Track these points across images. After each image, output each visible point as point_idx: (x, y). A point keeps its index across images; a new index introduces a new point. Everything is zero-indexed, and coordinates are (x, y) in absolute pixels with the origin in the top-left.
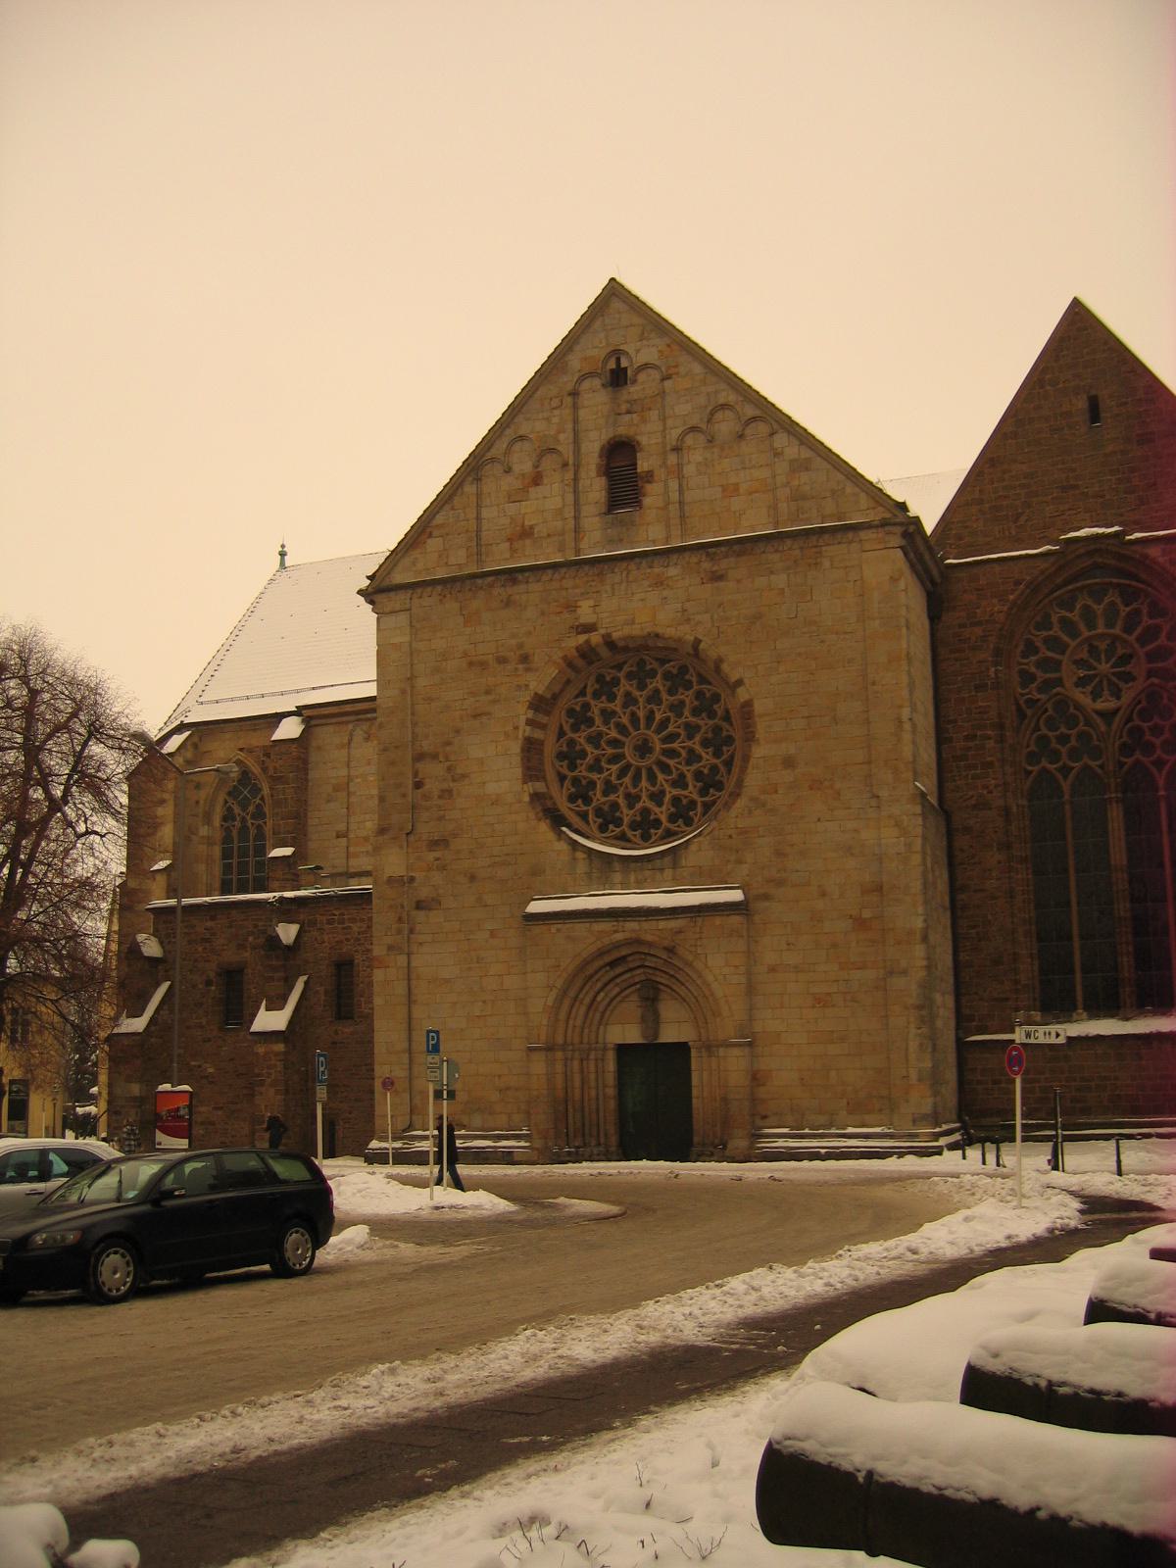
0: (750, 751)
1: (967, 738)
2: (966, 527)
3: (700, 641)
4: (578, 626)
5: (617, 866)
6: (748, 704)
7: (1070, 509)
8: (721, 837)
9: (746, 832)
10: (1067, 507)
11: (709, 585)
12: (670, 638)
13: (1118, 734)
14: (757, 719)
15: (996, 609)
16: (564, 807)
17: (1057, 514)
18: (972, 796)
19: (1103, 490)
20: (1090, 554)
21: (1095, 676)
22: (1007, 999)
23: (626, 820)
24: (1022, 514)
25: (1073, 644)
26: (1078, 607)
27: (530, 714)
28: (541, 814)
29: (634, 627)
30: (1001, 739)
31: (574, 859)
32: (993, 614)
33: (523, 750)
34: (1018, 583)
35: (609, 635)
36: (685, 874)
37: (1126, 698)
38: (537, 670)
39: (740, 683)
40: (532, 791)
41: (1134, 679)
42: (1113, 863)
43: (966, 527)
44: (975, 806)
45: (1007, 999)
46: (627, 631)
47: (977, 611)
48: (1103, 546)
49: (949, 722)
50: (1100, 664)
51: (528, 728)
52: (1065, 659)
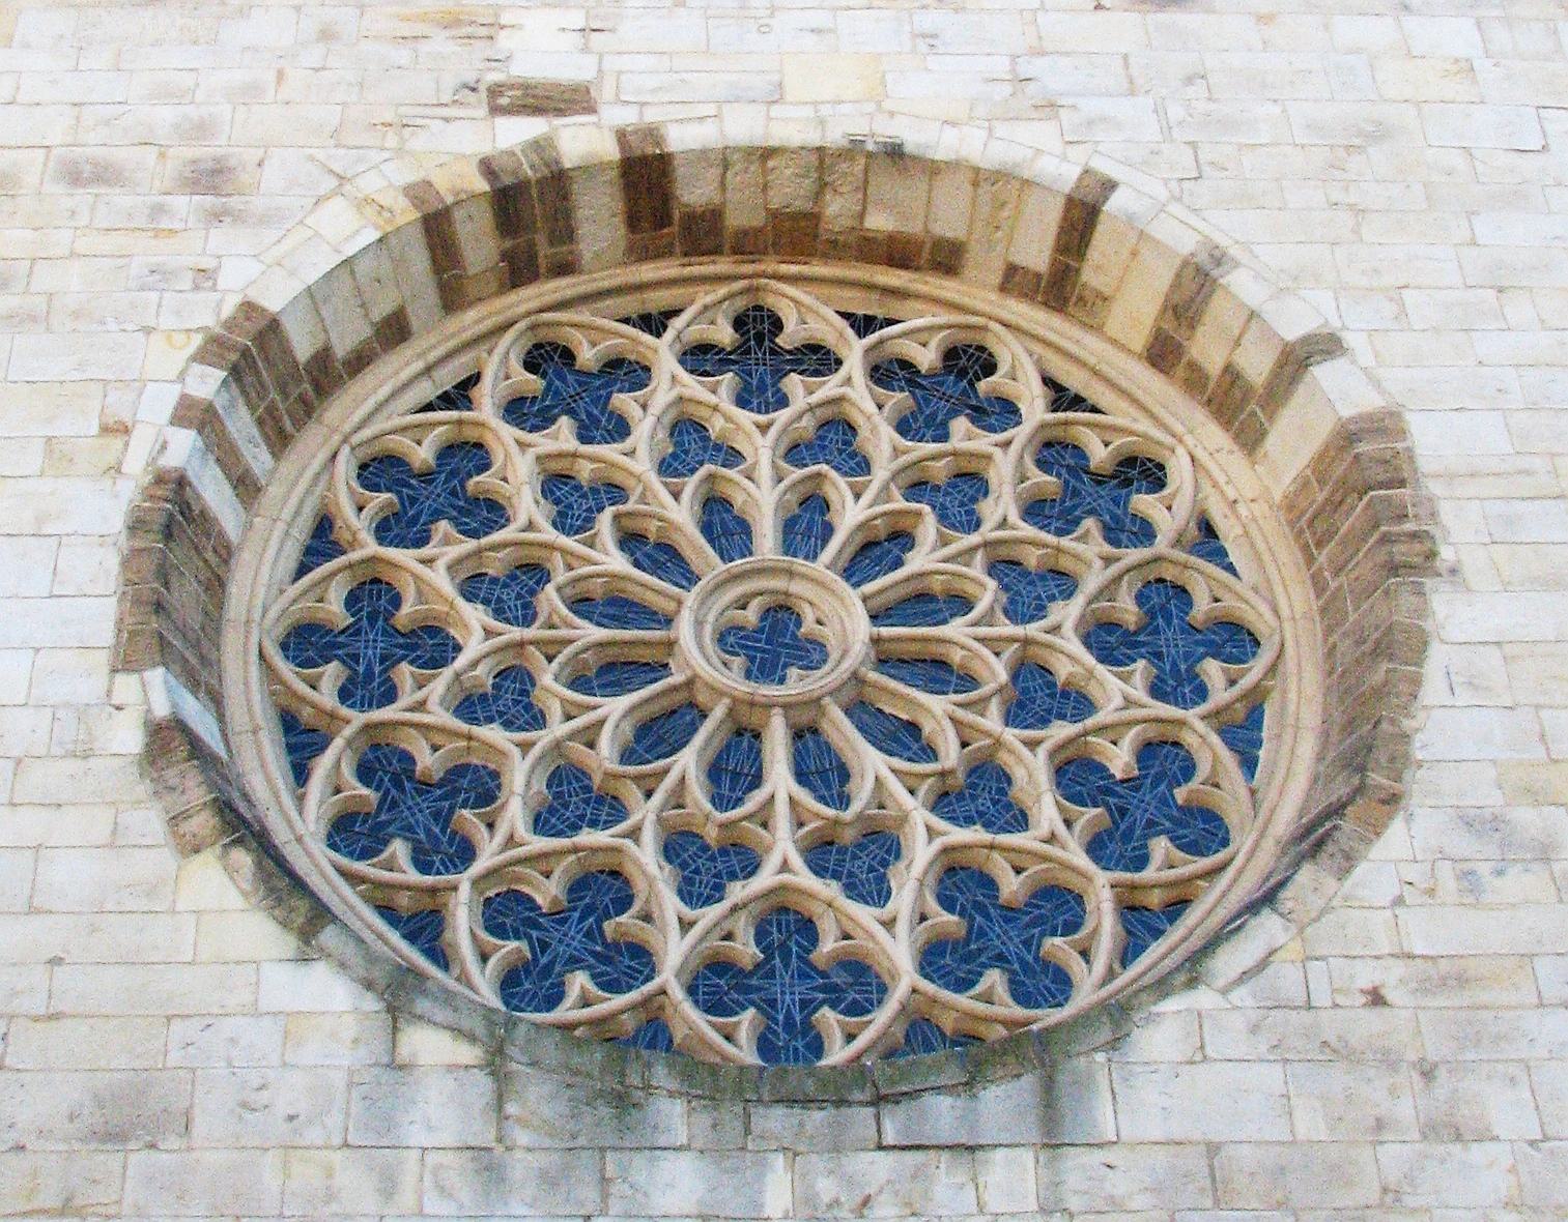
0: (1422, 612)
3: (1109, 186)
4: (495, 91)
5: (672, 1115)
6: (1384, 425)
8: (1321, 998)
9: (1463, 981)
11: (1133, 17)
12: (954, 166)
14: (1435, 488)
16: (315, 860)
23: (674, 953)
27: (207, 383)
28: (204, 823)
29: (775, 111)
31: (396, 1066)
33: (136, 526)
35: (652, 133)
36: (1118, 1185)
38: (264, 220)
39: (1325, 346)
40: (161, 710)
46: (744, 127)
51: (183, 447)
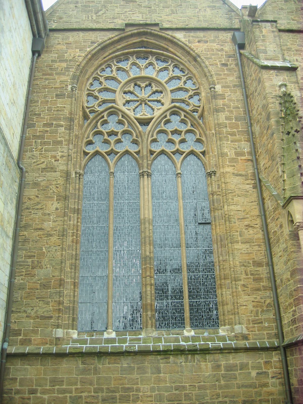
1: (45, 125)
2: (66, 13)
7: (129, 11)
10: (128, 10)
13: (151, 133)
15: (77, 55)
17: (122, 12)
18: (43, 162)
19: (151, 5)
20: (139, 34)
21: (138, 101)
22: (51, 317)
24: (101, 10)
25: (123, 82)
26: (130, 63)
30: (70, 128)
32: (74, 57)
34: (93, 43)
37: (157, 114)
41: (163, 104)
42: (142, 217)
43: (66, 13)
44: (44, 170)
45: (51, 317)
47: (65, 54)
48: (149, 31)
49: (35, 114)
50: (141, 94)
52: (118, 90)
